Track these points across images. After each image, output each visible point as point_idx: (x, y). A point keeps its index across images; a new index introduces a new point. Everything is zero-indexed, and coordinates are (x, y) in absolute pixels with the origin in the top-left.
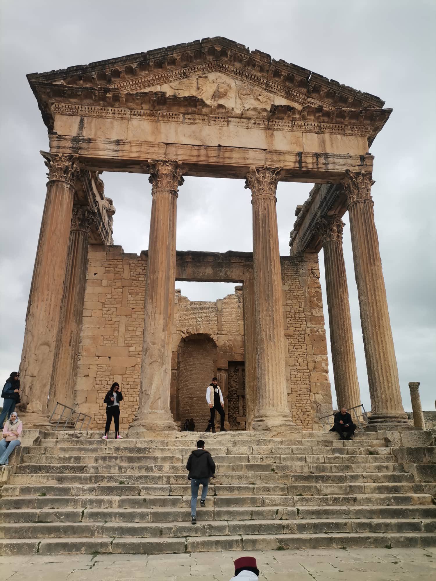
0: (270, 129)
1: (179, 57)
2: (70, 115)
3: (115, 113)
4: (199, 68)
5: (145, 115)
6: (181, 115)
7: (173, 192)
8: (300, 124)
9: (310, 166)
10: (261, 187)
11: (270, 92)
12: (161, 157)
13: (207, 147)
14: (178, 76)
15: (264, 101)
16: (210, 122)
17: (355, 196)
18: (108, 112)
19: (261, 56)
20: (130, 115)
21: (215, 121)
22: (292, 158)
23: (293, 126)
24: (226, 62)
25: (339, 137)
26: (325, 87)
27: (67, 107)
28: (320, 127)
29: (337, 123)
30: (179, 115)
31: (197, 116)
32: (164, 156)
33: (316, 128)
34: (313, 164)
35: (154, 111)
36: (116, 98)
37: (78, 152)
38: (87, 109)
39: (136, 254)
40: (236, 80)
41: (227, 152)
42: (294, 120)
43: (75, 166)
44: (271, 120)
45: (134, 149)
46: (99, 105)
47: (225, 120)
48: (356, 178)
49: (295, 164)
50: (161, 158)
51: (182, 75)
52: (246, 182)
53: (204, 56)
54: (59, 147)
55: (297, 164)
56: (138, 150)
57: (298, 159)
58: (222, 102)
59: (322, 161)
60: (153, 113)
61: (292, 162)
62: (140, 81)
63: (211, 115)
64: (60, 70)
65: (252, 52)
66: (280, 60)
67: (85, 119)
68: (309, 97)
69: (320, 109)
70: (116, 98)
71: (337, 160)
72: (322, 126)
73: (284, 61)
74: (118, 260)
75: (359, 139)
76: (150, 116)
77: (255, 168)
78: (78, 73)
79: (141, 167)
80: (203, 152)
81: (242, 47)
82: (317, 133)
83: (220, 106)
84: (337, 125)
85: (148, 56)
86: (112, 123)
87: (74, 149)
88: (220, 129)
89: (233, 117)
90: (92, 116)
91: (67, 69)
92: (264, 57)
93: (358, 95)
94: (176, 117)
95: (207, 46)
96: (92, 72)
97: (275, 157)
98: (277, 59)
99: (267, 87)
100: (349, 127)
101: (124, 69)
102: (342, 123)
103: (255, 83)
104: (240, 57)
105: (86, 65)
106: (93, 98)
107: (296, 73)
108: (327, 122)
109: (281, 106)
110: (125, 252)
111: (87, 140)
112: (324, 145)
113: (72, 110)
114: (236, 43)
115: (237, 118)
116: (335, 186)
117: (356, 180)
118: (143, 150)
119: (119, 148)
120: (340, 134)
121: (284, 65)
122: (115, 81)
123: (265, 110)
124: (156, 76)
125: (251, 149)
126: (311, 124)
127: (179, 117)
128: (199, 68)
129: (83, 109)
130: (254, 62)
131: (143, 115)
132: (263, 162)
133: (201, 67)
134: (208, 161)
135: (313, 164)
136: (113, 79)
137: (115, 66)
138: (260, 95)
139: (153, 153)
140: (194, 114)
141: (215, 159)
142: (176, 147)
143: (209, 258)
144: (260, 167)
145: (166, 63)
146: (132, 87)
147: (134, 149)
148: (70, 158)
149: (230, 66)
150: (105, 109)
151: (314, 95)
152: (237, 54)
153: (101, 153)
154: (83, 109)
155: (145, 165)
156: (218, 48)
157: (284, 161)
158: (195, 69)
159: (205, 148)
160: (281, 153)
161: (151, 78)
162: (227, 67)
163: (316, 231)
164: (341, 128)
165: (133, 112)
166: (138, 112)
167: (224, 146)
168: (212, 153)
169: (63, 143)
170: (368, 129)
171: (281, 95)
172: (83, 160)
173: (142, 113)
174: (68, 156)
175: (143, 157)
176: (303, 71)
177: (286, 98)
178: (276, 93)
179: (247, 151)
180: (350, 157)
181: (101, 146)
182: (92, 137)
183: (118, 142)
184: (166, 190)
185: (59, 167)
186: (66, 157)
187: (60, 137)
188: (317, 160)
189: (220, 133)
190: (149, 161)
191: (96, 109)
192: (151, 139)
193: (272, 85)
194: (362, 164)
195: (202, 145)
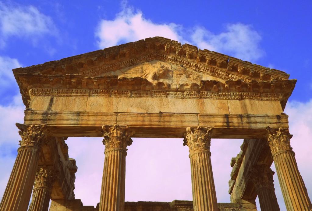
1: (128, 52)
3: (77, 93)
5: (101, 93)
7: (122, 151)
9: (236, 125)
10: (196, 144)
13: (150, 114)
15: (195, 78)
17: (277, 148)
19: (189, 47)
22: (221, 119)
24: (164, 53)
25: (257, 102)
26: (241, 66)
27: (41, 90)
29: (254, 91)
30: (128, 91)
31: (142, 92)
32: (116, 122)
34: (239, 123)
35: (108, 90)
36: (79, 83)
37: (46, 122)
38: (56, 91)
39: (93, 206)
40: (172, 65)
41: (167, 118)
44: (201, 92)
45: (91, 118)
46: (66, 88)
50: (113, 124)
51: (131, 63)
52: (184, 140)
54: (32, 120)
55: (225, 124)
56: (95, 118)
59: (245, 121)
61: (220, 122)
62: (98, 69)
63: (153, 90)
64: (39, 65)
65: (183, 45)
66: (205, 49)
67: (55, 98)
68: (230, 74)
70: (79, 83)
71: (258, 120)
73: (208, 50)
75: (273, 102)
76: (105, 93)
78: (52, 66)
80: (147, 118)
82: (239, 100)
83: (160, 84)
85: (104, 52)
87: (43, 120)
88: (161, 100)
90: (61, 96)
91: (44, 64)
92: (192, 48)
96: (62, 65)
97: (206, 119)
98: (203, 49)
99: (196, 68)
100: (264, 94)
101: (86, 62)
102: (258, 91)
103: (187, 66)
105: (58, 61)
106: (62, 82)
107: (217, 58)
109: (208, 81)
110: (84, 205)
111: (54, 113)
112: (246, 108)
114: (171, 40)
116: (260, 140)
118: (98, 118)
119: (79, 118)
125: (187, 114)
127: (128, 93)
131: (99, 93)
132: (197, 124)
134: (151, 125)
135: (239, 123)
137: (80, 59)
138: (191, 74)
139: (106, 121)
140: (139, 90)
141: (157, 123)
142: (125, 115)
144: (195, 128)
145: (118, 56)
146: (92, 73)
147: (91, 118)
150: (70, 90)
153: (65, 122)
154: (54, 91)
156: (158, 45)
157: (215, 122)
158: (140, 59)
159: (148, 115)
160: (211, 116)
161: (107, 67)
162: (164, 56)
163: (249, 179)
165: (92, 91)
166: (95, 91)
168: (156, 118)
169: (35, 117)
170: (279, 95)
171: (208, 74)
174: (38, 126)
175: (98, 124)
176: (223, 56)
177: (212, 75)
179: (183, 115)
180: (268, 117)
181: (66, 117)
182: (58, 111)
183: (78, 114)
185: (30, 135)
186: (37, 127)
187: (33, 112)
189: (161, 103)
190: (103, 127)
191: (64, 90)
192: (104, 110)
193: (200, 67)
194: (279, 122)
195: (146, 112)
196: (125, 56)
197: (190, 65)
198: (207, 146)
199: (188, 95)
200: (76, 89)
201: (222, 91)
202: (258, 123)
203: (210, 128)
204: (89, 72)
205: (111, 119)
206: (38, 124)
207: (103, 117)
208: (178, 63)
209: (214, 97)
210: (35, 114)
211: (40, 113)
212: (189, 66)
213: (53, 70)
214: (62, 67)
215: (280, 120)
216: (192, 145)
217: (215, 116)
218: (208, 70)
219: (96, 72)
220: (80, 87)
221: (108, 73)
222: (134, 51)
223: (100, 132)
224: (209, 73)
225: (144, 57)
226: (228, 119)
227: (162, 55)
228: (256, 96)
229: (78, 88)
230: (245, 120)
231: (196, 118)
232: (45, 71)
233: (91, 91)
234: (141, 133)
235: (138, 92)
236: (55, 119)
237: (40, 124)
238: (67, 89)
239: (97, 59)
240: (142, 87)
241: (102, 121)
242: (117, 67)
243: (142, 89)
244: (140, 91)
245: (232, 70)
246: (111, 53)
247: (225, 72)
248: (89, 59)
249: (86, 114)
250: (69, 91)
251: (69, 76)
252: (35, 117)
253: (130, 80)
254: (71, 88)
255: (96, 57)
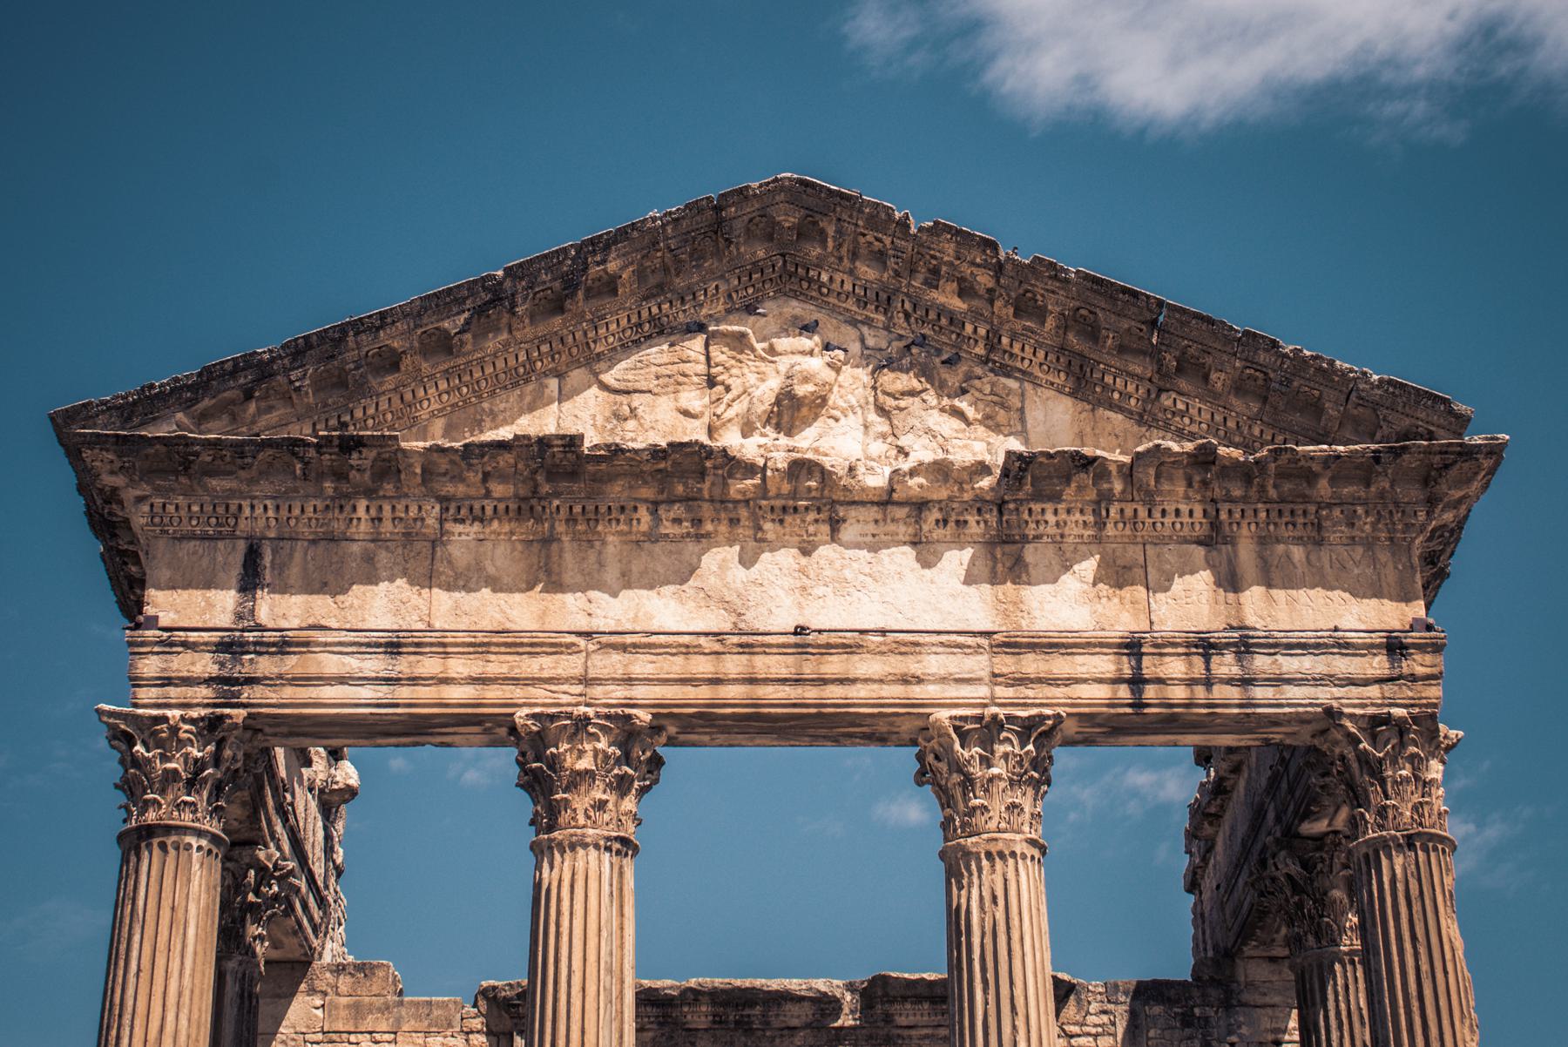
0: (1007, 540)
2: (205, 537)
4: (711, 290)
5: (500, 520)
6: (644, 514)
8: (1129, 512)
9: (1178, 693)
11: (1006, 371)
12: (566, 697)
14: (628, 332)
16: (760, 529)
18: (354, 516)
20: (441, 521)
21: (781, 521)
23: (1100, 525)
25: (1298, 553)
27: (195, 508)
28: (1215, 525)
30: (635, 509)
31: (706, 510)
32: (578, 689)
33: (1197, 527)
35: (534, 502)
37: (239, 694)
38: (271, 513)
40: (865, 330)
41: (830, 658)
42: (1105, 498)
43: (228, 753)
44: (1012, 506)
46: (320, 494)
47: (821, 516)
48: (1374, 739)
49: (1115, 692)
50: (565, 699)
52: (920, 757)
53: (732, 248)
54: (167, 681)
55: (1124, 692)
57: (1126, 666)
58: (806, 441)
60: (532, 508)
63: (764, 503)
69: (1204, 459)
71: (1291, 664)
72: (1223, 516)
74: (378, 1037)
77: (947, 723)
78: (242, 381)
79: (486, 731)
81: (883, 216)
83: (801, 468)
84: (1287, 508)
85: (508, 284)
86: (369, 559)
87: (225, 683)
89: (854, 503)
93: (1361, 386)
94: (622, 517)
95: (739, 213)
96: (294, 369)
97: (1032, 664)
100: (1337, 512)
101: (416, 344)
102: (1306, 499)
103: (944, 339)
104: (876, 243)
106: (298, 472)
108: (1245, 499)
111: (274, 644)
113: (213, 521)
115: (872, 503)
117: (1374, 746)
119: (403, 665)
120: (1299, 540)
121: (1055, 278)
122: (381, 384)
123: (982, 469)
124: (543, 342)
126: (1178, 513)
127: (637, 516)
128: (711, 290)
129: (259, 517)
130: (934, 262)
131: (492, 519)
133: (723, 288)
135: (1191, 682)
136: (373, 382)
140: (695, 499)
142: (624, 648)
143: (790, 1008)
146: (445, 397)
148: (212, 726)
149: (838, 277)
150: (341, 507)
151: (1183, 384)
152: (864, 235)
154: (259, 511)
155: (500, 726)
156: (788, 218)
158: (694, 298)
161: (522, 357)
162: (825, 277)
164: (1301, 520)
165: (452, 511)
166: (471, 509)
167: (820, 631)
169: (183, 664)
171: (1052, 384)
172: (256, 725)
173: (489, 511)
174: (202, 719)
177: (1073, 394)
178: (1031, 374)
180: (1344, 647)
183: (393, 648)
184: (588, 840)
186: (193, 721)
188: (1208, 669)
193: (1011, 346)
195: (727, 627)
196: (614, 292)
197: (958, 335)
198: (1027, 809)
199: (945, 522)
200: (370, 498)
201: (1119, 501)
202: (1289, 681)
203: (1048, 717)
204: (432, 391)
205: (560, 671)
206: (198, 705)
207: (517, 658)
208: (900, 319)
209: (1076, 531)
210: (180, 649)
211: (206, 644)
212: (954, 336)
213: (248, 395)
214: (292, 382)
215: (1404, 664)
216: (956, 804)
217: (1075, 645)
218: (1051, 362)
219: (465, 390)
220: (389, 488)
221: (530, 387)
222: (663, 257)
223: (503, 731)
224: (1057, 381)
225: (717, 287)
226: (1139, 662)
227: (811, 273)
228: (1294, 525)
229: (381, 493)
230: (1225, 665)
231: (980, 658)
232: (206, 403)
233: (447, 509)
234: (706, 733)
235: (689, 509)
236: (280, 677)
237: (207, 705)
238: (328, 502)
239: (468, 322)
240: (706, 486)
241: (515, 681)
242: (575, 351)
243: (706, 495)
244: (696, 503)
245: (1180, 370)
246: (545, 282)
247: (1140, 378)
248: (431, 326)
249: (432, 645)
250: (337, 511)
251: (336, 442)
252: (183, 664)
253: (645, 456)
254: (348, 496)
255: (466, 315)
